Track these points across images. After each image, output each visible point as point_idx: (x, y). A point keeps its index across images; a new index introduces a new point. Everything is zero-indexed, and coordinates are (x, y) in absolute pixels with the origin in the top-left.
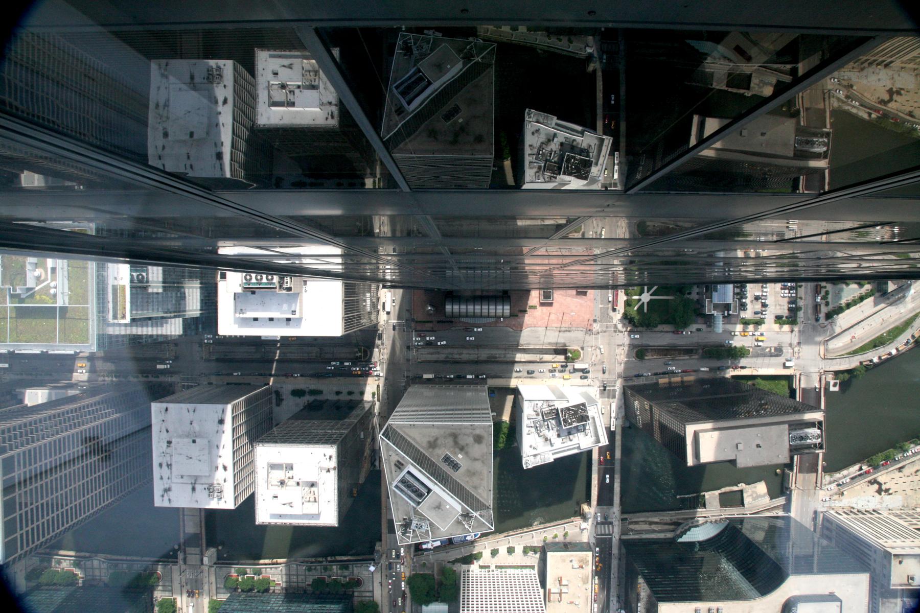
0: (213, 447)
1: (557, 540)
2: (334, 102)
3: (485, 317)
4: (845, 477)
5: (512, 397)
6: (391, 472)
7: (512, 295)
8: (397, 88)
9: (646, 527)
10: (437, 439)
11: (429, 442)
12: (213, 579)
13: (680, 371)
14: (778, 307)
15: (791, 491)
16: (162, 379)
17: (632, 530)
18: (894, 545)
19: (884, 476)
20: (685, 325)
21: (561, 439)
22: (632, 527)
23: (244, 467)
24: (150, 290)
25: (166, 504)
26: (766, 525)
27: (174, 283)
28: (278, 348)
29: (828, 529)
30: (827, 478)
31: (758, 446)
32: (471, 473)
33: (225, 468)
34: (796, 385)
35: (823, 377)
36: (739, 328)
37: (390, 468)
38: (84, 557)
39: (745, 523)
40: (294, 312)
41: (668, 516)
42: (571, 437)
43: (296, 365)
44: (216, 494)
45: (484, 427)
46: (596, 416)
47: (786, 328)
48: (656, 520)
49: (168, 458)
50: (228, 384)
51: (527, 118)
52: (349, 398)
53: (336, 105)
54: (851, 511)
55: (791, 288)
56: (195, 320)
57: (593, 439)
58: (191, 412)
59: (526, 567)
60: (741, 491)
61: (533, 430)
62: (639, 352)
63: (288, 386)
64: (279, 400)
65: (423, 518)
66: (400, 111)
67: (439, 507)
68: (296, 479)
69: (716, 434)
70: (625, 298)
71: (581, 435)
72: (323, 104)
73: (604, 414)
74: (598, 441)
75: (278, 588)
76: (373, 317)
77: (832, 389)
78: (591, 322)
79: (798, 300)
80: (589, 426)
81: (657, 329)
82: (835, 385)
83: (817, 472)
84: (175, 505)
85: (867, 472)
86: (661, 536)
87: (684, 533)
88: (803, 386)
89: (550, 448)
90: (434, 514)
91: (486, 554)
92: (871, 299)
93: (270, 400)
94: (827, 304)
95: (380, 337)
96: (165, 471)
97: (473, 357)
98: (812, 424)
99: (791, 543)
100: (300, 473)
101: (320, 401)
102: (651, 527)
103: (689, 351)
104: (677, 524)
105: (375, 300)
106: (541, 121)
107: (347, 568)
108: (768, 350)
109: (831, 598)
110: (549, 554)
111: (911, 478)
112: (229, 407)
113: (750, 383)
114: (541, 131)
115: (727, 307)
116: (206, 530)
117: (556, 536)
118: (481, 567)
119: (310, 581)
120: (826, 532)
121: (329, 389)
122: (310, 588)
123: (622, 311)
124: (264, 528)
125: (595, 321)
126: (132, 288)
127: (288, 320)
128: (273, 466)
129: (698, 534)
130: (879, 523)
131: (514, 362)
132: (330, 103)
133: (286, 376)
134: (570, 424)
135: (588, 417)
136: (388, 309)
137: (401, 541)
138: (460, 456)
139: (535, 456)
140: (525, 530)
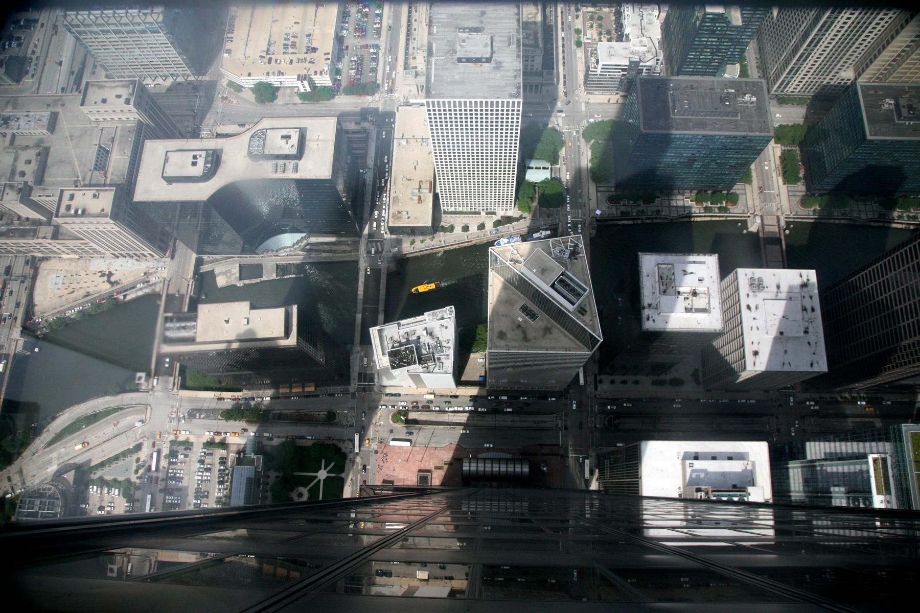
1: (421, 238)
3: (489, 459)
4: (141, 289)
7: (459, 481)
10: (544, 336)
11: (550, 333)
12: (750, 203)
17: (348, 245)
18: (105, 226)
20: (283, 444)
23: (732, 309)
25: (805, 272)
27: (821, 497)
29: (163, 241)
30: (157, 289)
33: (749, 307)
34: (178, 380)
38: (875, 221)
44: (756, 282)
45: (496, 347)
46: (381, 356)
49: (806, 317)
50: (748, 391)
52: (625, 378)
54: (139, 257)
56: (793, 458)
57: (384, 334)
58: (786, 362)
59: (451, 213)
60: (241, 279)
61: (444, 344)
64: (695, 375)
65: (559, 259)
71: (396, 338)
74: (380, 332)
75: (687, 195)
77: (143, 375)
79: (166, 466)
82: (140, 378)
83: (168, 295)
88: (172, 379)
91: (489, 226)
92: (92, 464)
96: (808, 304)
107: (622, 213)
108: (203, 416)
109: (170, 180)
110: (429, 224)
111: (80, 285)
118: (494, 213)
119: (657, 201)
122: (658, 194)
125: (376, 452)
126: (870, 492)
128: (704, 311)
130: (115, 246)
138: (520, 319)
139: (442, 318)
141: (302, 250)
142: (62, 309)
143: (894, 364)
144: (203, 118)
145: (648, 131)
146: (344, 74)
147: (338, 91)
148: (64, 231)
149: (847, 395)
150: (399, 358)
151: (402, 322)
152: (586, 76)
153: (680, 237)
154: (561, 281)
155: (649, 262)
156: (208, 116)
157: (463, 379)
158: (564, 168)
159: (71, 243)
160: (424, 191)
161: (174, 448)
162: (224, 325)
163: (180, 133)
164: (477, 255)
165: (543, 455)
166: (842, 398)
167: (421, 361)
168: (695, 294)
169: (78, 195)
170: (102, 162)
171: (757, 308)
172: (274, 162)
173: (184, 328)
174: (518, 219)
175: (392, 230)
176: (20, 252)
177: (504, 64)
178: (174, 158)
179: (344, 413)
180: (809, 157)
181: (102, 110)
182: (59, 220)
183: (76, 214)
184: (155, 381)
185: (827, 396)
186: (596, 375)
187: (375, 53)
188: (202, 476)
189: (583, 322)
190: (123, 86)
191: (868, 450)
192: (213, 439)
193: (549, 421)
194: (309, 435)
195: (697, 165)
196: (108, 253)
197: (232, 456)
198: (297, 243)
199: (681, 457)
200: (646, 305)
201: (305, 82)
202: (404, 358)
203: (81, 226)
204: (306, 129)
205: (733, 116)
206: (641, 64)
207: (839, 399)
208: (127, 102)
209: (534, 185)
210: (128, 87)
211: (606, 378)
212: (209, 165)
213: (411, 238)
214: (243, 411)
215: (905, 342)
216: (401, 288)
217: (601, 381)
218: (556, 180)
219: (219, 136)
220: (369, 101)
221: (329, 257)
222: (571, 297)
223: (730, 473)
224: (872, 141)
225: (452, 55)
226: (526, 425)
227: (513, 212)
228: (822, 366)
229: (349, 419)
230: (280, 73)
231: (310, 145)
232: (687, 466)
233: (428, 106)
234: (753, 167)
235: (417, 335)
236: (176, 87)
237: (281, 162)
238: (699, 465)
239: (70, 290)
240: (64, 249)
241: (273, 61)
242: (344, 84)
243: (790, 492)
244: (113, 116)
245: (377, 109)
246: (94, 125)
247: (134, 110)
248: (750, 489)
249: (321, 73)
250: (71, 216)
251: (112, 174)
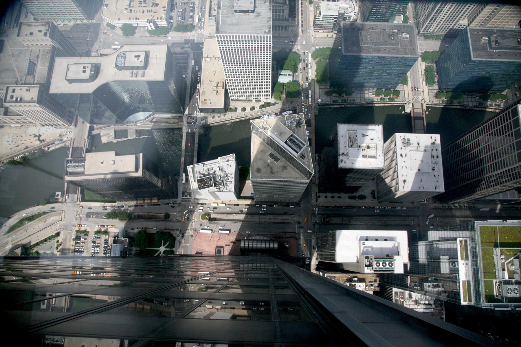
1: (218, 115)
4: (58, 144)
6: (307, 153)
11: (286, 169)
12: (406, 96)
17: (177, 119)
18: (34, 108)
20: (140, 232)
25: (433, 136)
26: (104, 120)
31: (102, 163)
33: (401, 155)
34: (80, 196)
38: (477, 107)
44: (406, 141)
45: (256, 177)
46: (193, 182)
49: (434, 162)
50: (402, 203)
54: (56, 126)
58: (422, 186)
61: (229, 175)
64: (373, 193)
65: (290, 127)
71: (202, 172)
74: (193, 168)
77: (60, 193)
79: (74, 244)
82: (58, 195)
83: (73, 148)
84: (429, 135)
88: (76, 195)
92: (32, 244)
96: (435, 154)
99: (91, 109)
108: (94, 216)
109: (71, 81)
127: (367, 240)
128: (374, 157)
130: (42, 119)
135: (198, 182)
137: (302, 115)
138: (269, 161)
139: (228, 161)
141: (151, 121)
142: (12, 156)
143: (481, 188)
144: (92, 46)
145: (347, 54)
146: (175, 19)
147: (171, 29)
148: (11, 111)
149: (457, 205)
150: (203, 183)
151: (206, 163)
152: (314, 21)
153: (364, 115)
154: (291, 140)
155: (343, 129)
156: (96, 43)
157: (242, 195)
158: (301, 75)
160: (219, 88)
161: (79, 234)
162: (104, 165)
163: (79, 53)
164: (245, 125)
165: (286, 238)
166: (454, 206)
167: (216, 185)
168: (368, 147)
169: (18, 89)
170: (31, 70)
171: (406, 156)
172: (131, 71)
173: (78, 166)
174: (274, 104)
175: (202, 110)
177: (261, 14)
178: (72, 68)
179: (174, 214)
180: (438, 68)
181: (30, 39)
182: (6, 104)
183: (16, 101)
184: (67, 197)
185: (446, 205)
186: (316, 193)
187: (192, 7)
188: (94, 250)
190: (43, 25)
191: (458, 236)
193: (289, 219)
194: (153, 227)
195: (376, 74)
197: (112, 239)
198: (148, 117)
199: (358, 239)
200: (341, 153)
201: (151, 24)
202: (206, 183)
204: (149, 52)
205: (396, 45)
206: (346, 15)
207: (453, 207)
208: (45, 34)
209: (283, 85)
210: (45, 26)
211: (323, 195)
212: (93, 73)
213: (213, 115)
214: (117, 214)
215: (487, 176)
216: (209, 143)
217: (319, 197)
218: (295, 82)
219: (102, 55)
220: (189, 35)
221: (165, 126)
222: (297, 150)
223: (385, 248)
224: (474, 61)
225: (231, 8)
226: (276, 221)
227: (271, 100)
228: (442, 189)
229: (177, 218)
230: (137, 19)
231: (152, 61)
232: (361, 244)
233: (218, 38)
234: (408, 74)
235: (214, 170)
236: (76, 26)
237: (135, 71)
238: (368, 243)
239: (16, 145)
240: (11, 121)
241: (133, 11)
242: (175, 25)
243: (418, 259)
244: (37, 43)
245: (194, 40)
246: (26, 48)
247: (50, 39)
248: (396, 257)
249: (161, 19)
250: (14, 102)
251: (38, 77)
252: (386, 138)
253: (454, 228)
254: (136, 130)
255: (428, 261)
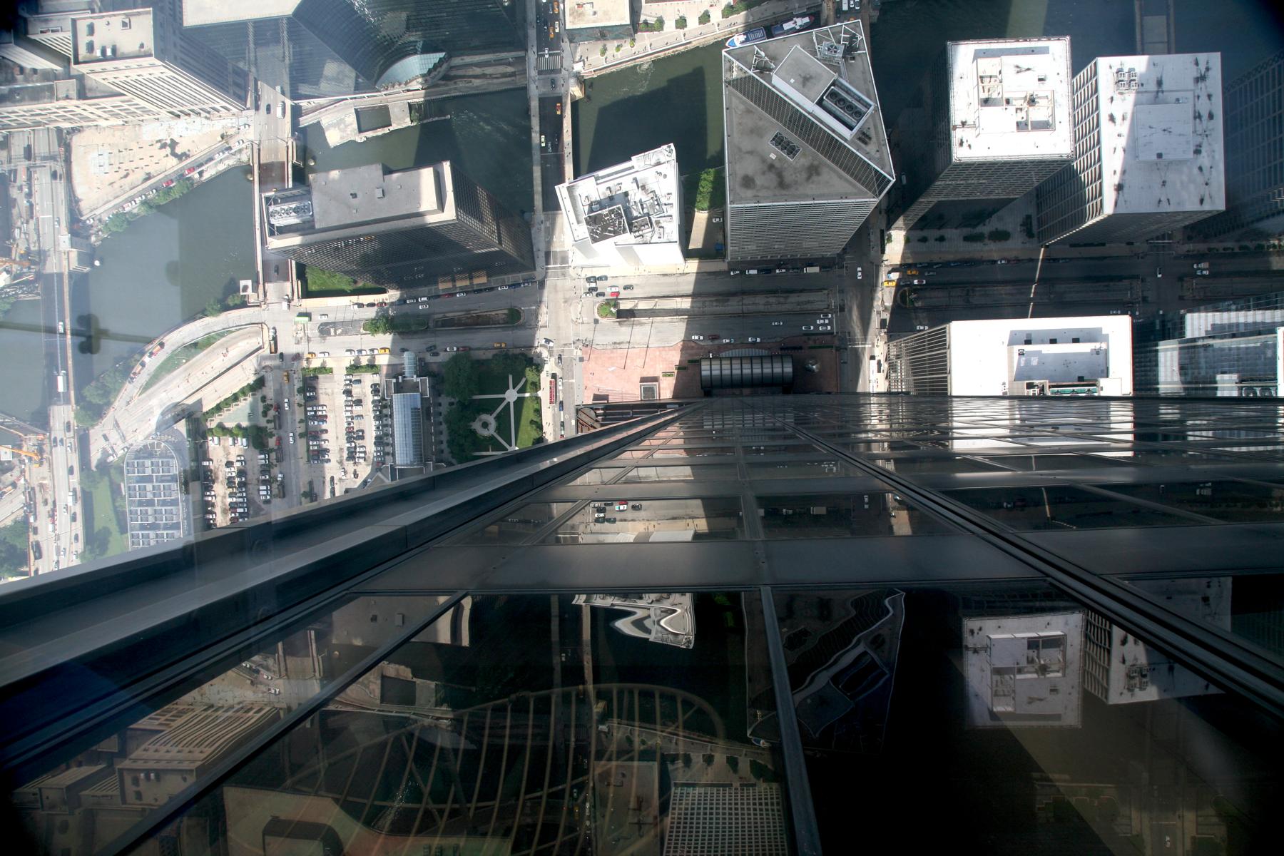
0: (1132, 151)
1: (616, 43)
2: (970, 653)
3: (736, 358)
5: (691, 247)
6: (876, 127)
7: (699, 390)
8: (883, 674)
9: (489, 71)
10: (809, 178)
11: (818, 174)
13: (455, 296)
14: (329, 391)
15: (293, 134)
16: (1202, 247)
17: (509, 64)
18: (151, 70)
19: (169, 166)
20: (455, 360)
21: (623, 190)
22: (510, 69)
24: (1235, 377)
25: (1202, 57)
26: (324, 85)
28: (1031, 300)
29: (238, 85)
30: (244, 158)
31: (354, 196)
32: (756, 132)
33: (1112, 118)
34: (298, 285)
35: (261, 298)
36: (383, 360)
37: (877, 133)
39: (352, 84)
40: (1021, 354)
41: (461, 88)
42: (608, 194)
43: (999, 277)
44: (1126, 78)
45: (741, 200)
46: (575, 225)
47: (316, 364)
48: (477, 82)
50: (1103, 245)
51: (692, 638)
52: (925, 233)
53: (967, 648)
54: (209, 113)
55: (316, 417)
56: (1166, 336)
57: (577, 192)
60: (360, 131)
61: (663, 200)
62: (519, 319)
63: (1016, 246)
65: (828, 61)
66: (877, 642)
67: (805, 81)
68: (1011, 109)
69: (422, 209)
70: (540, 393)
72: (986, 648)
73: (569, 231)
74: (570, 189)
76: (894, 352)
77: (249, 283)
78: (586, 358)
79: (302, 402)
80: (584, 210)
81: (495, 352)
82: (245, 288)
83: (260, 166)
84: (1188, 58)
85: (191, 169)
86: (468, 59)
87: (436, 66)
88: (288, 284)
89: (638, 176)
90: (809, 71)
91: (716, 15)
92: (205, 409)
93: (1040, 222)
94: (264, 399)
95: (883, 323)
96: (1204, 107)
97: (748, 300)
98: (284, 231)
99: (287, 61)
100: (1009, 117)
101: (966, 226)
102: (483, 71)
103: (447, 324)
104: (447, 78)
105: (893, 375)
106: (671, 637)
108: (339, 331)
110: (626, 20)
111: (133, 166)
112: (1108, 209)
113: (360, 284)
114: (673, 622)
115: (399, 388)
116: (1133, 23)
117: (618, 48)
120: (240, 81)
121: (955, 245)
123: (543, 375)
124: (1051, 31)
125: (581, 359)
126: (1276, 379)
127: (1028, 342)
128: (1045, 126)
129: (415, 66)
131: (693, 295)
132: (976, 651)
133: (1018, 260)
134: (612, 211)
135: (588, 223)
136: (874, 363)
137: (856, 25)
138: (773, 156)
139: (658, 164)
140: (662, 55)
148: (94, 84)
151: (601, 173)
159: (107, 103)
176: (38, 124)
183: (104, 58)
189: (867, 154)
192: (357, 359)
196: (163, 111)
202: (609, 225)
203: (116, 74)
240: (99, 112)
252: (1076, 67)
253: (1268, 304)
254: (410, 105)
255: (1185, 389)
